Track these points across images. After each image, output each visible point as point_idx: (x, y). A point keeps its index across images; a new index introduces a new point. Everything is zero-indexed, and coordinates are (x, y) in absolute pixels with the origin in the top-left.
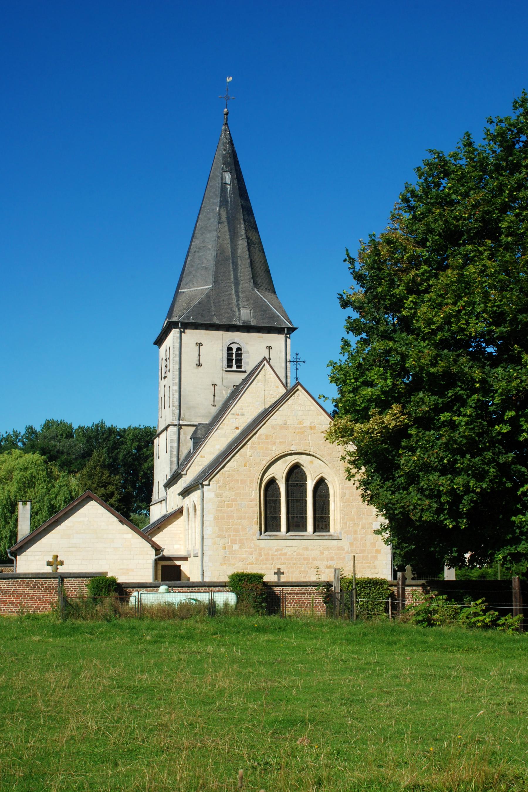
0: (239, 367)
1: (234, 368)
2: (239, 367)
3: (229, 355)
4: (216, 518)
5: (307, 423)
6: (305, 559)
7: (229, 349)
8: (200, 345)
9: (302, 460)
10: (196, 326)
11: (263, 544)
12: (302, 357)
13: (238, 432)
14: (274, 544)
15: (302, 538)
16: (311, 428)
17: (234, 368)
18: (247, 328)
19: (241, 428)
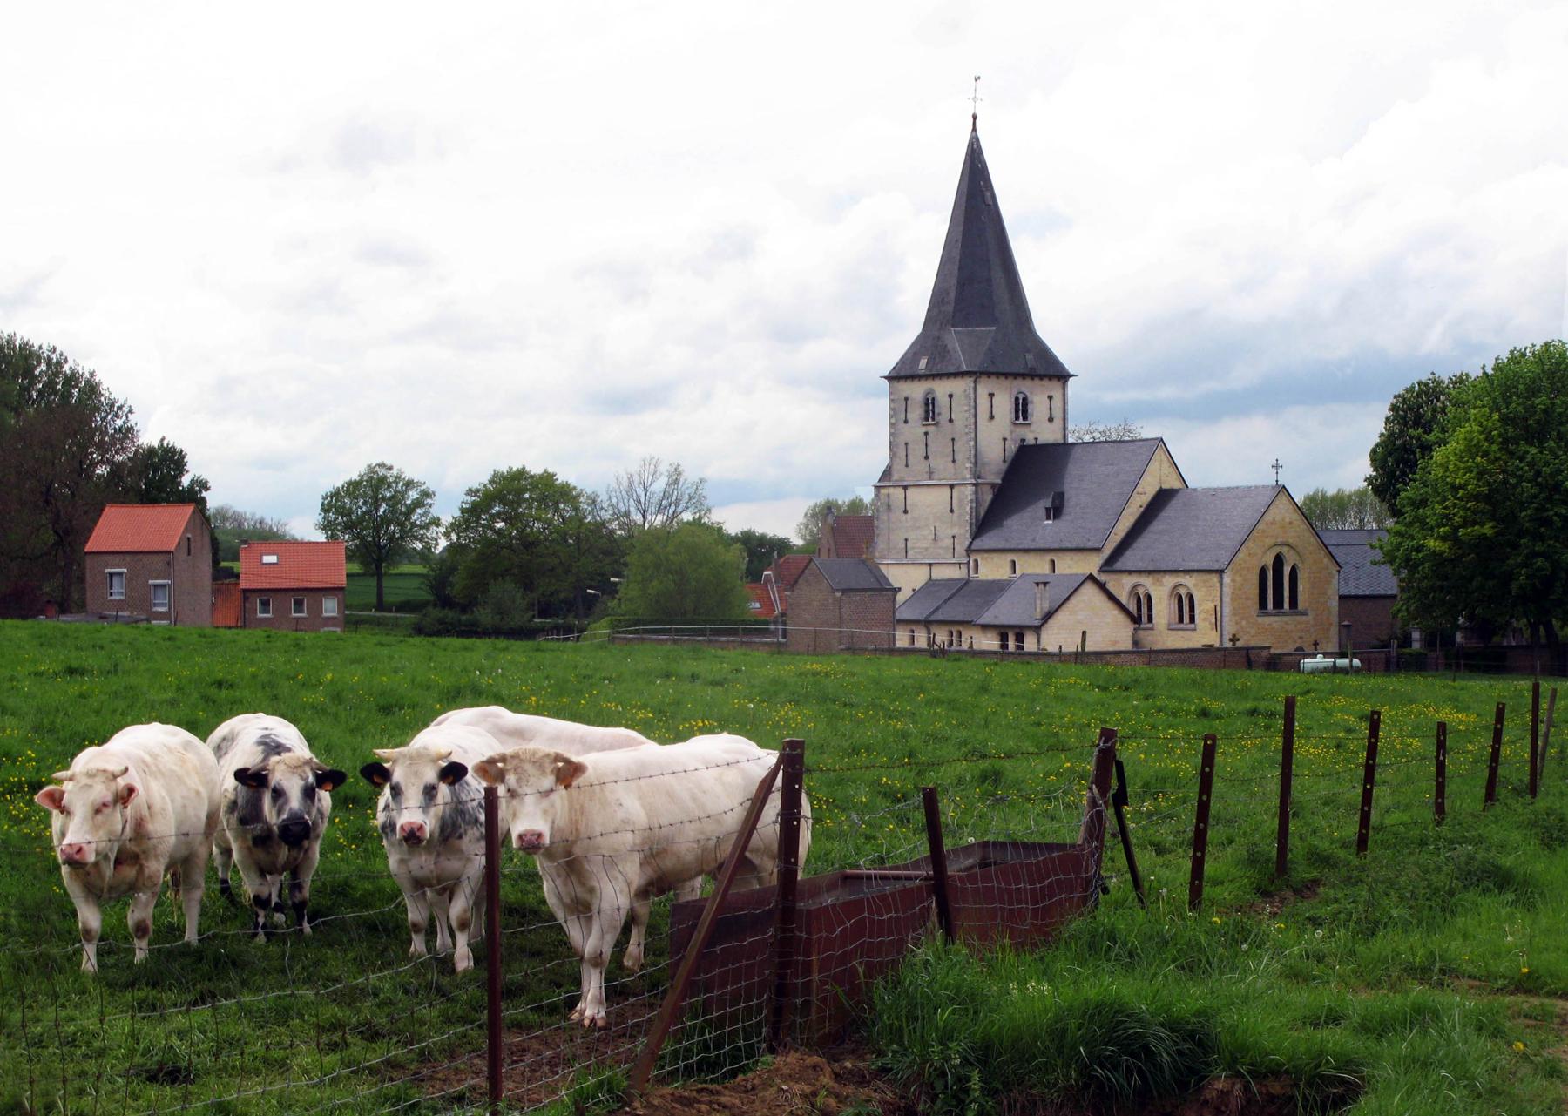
0: (1025, 418)
1: (1021, 421)
2: (1025, 418)
3: (1017, 405)
4: (1232, 599)
5: (1287, 520)
6: (1286, 631)
7: (1017, 399)
8: (991, 395)
9: (1284, 550)
10: (989, 374)
11: (1260, 620)
12: (1280, 463)
13: (1142, 509)
14: (1267, 620)
15: (1284, 614)
16: (1290, 523)
17: (1021, 421)
18: (1031, 375)
19: (1144, 506)
